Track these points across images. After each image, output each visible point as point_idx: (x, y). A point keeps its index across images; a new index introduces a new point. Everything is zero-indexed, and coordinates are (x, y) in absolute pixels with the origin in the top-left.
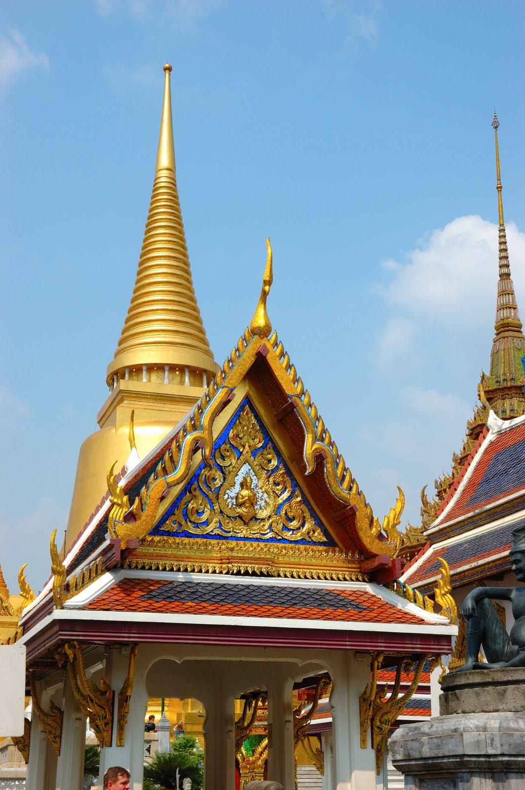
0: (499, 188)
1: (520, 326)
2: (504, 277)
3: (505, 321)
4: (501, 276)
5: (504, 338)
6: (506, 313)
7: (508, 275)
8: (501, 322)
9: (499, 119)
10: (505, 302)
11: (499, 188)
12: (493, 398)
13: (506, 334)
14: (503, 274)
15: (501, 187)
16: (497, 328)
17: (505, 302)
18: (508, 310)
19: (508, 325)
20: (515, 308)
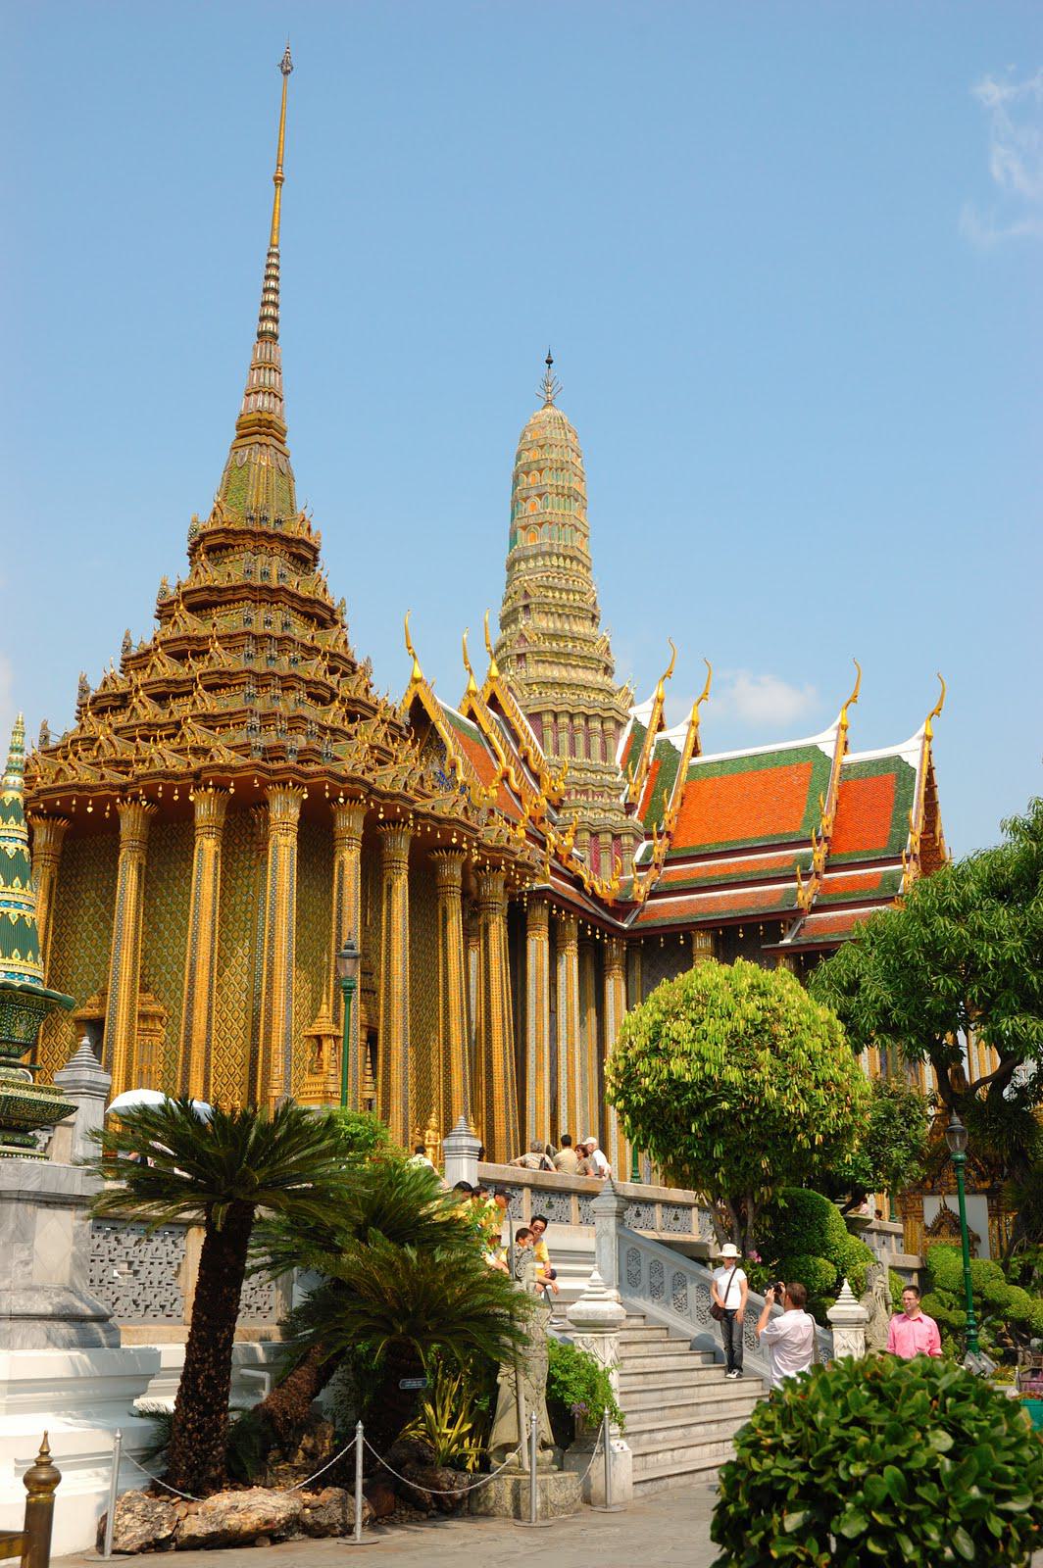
0: (278, 181)
1: (284, 433)
2: (268, 337)
3: (265, 416)
4: (261, 335)
5: (261, 445)
6: (263, 401)
7: (275, 336)
8: (258, 415)
9: (294, 61)
10: (267, 382)
11: (278, 181)
12: (233, 547)
13: (263, 439)
14: (265, 332)
15: (282, 179)
16: (239, 427)
17: (267, 382)
18: (266, 398)
19: (270, 424)
20: (281, 400)
